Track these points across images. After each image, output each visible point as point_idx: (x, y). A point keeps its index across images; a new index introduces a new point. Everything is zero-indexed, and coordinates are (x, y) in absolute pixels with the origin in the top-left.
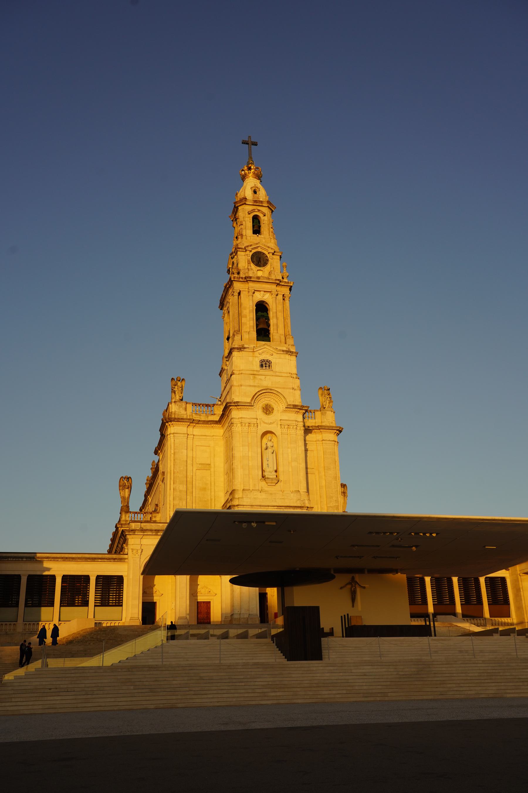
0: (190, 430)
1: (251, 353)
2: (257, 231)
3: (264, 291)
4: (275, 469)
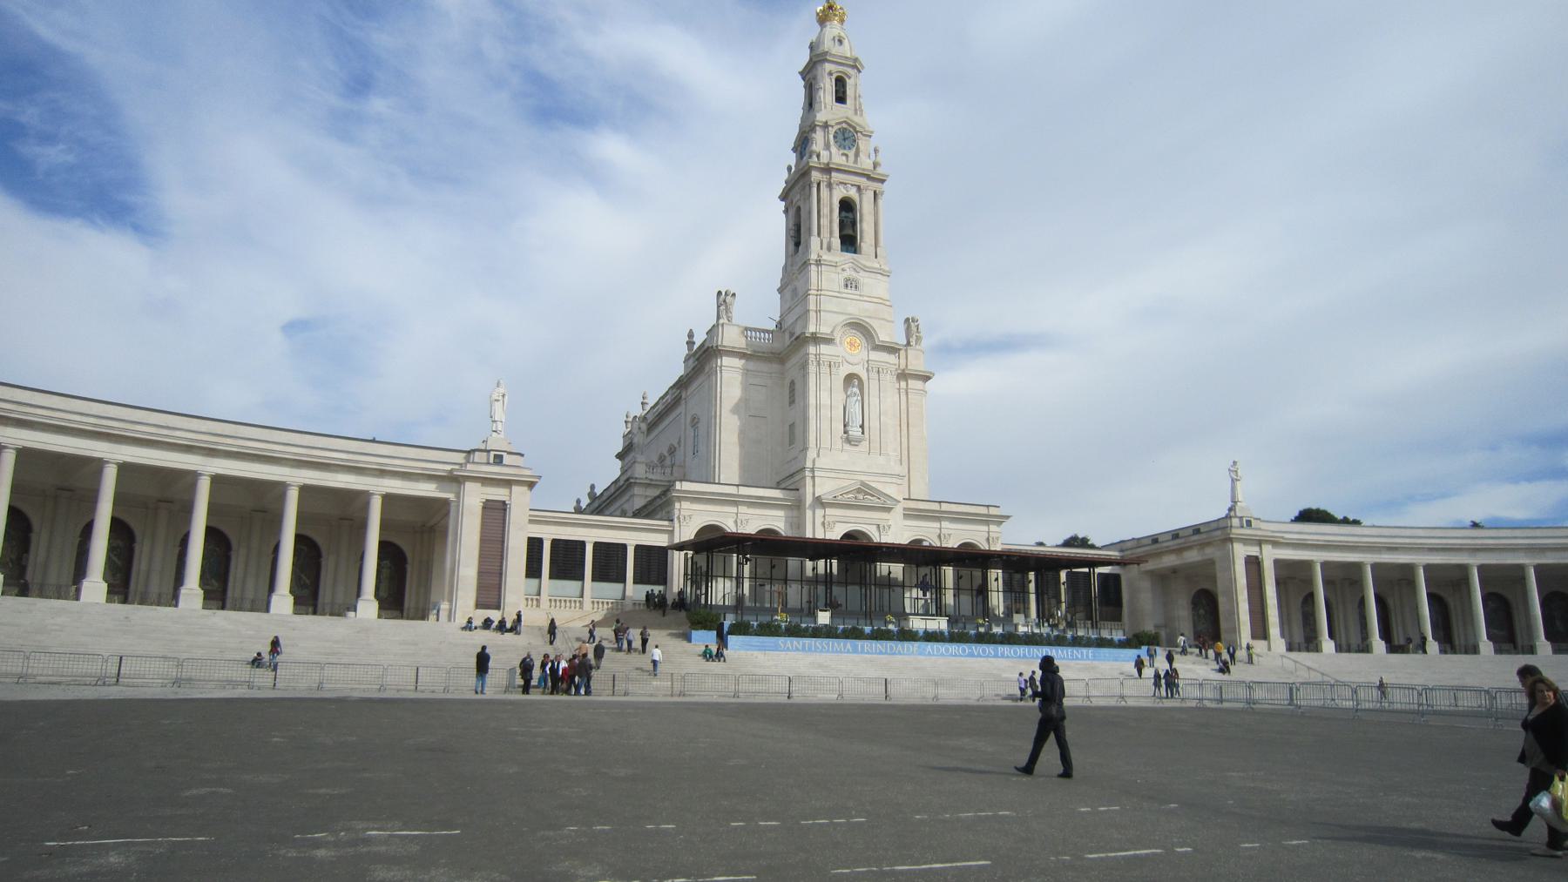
1: (834, 268)
2: (841, 98)
3: (852, 185)
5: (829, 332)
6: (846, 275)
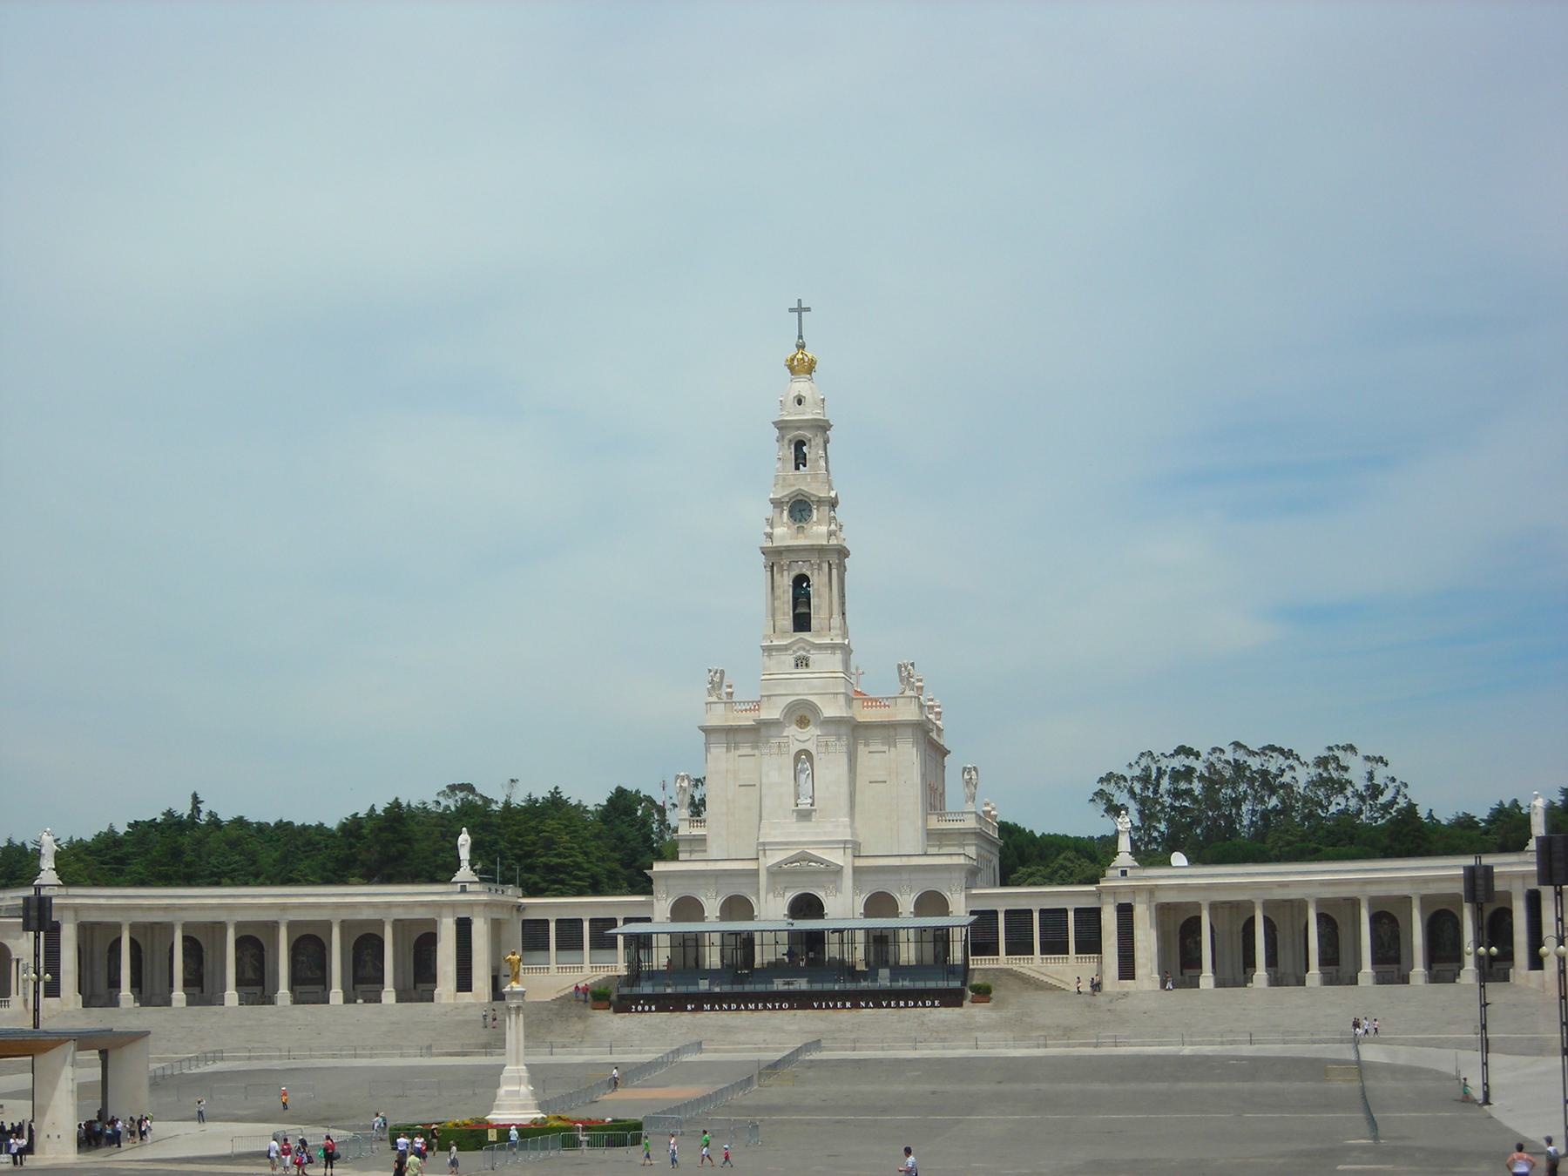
4: (811, 794)
5: (778, 717)
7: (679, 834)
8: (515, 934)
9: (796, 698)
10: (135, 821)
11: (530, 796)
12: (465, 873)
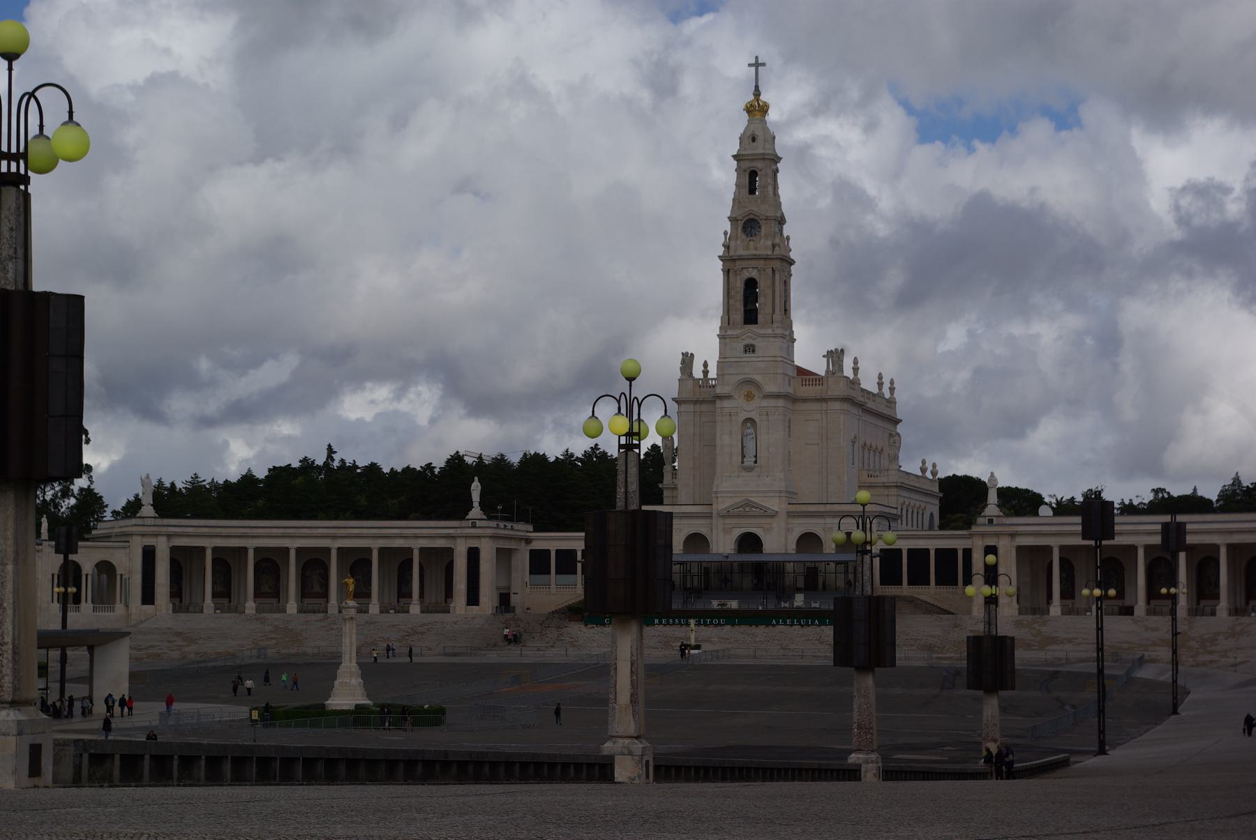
0: (698, 406)
4: (755, 454)
6: (745, 342)
7: (664, 483)
8: (522, 560)
9: (743, 377)
10: (274, 467)
11: (567, 451)
12: (476, 512)
